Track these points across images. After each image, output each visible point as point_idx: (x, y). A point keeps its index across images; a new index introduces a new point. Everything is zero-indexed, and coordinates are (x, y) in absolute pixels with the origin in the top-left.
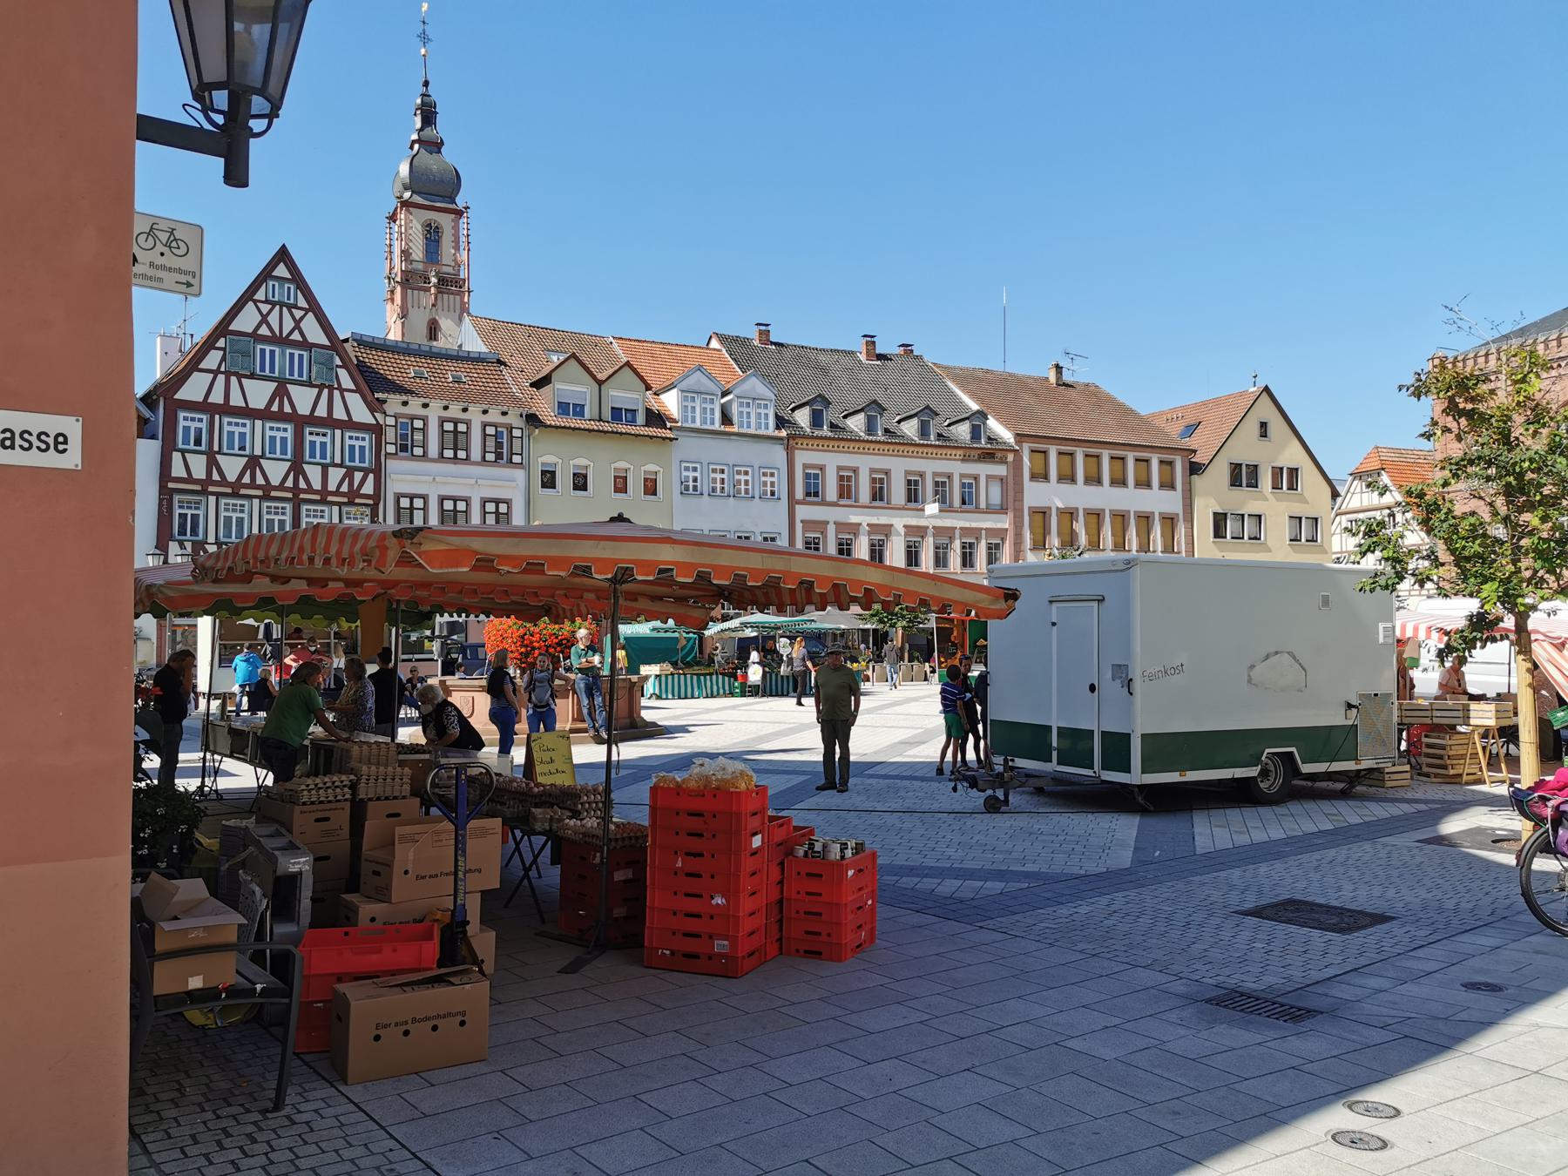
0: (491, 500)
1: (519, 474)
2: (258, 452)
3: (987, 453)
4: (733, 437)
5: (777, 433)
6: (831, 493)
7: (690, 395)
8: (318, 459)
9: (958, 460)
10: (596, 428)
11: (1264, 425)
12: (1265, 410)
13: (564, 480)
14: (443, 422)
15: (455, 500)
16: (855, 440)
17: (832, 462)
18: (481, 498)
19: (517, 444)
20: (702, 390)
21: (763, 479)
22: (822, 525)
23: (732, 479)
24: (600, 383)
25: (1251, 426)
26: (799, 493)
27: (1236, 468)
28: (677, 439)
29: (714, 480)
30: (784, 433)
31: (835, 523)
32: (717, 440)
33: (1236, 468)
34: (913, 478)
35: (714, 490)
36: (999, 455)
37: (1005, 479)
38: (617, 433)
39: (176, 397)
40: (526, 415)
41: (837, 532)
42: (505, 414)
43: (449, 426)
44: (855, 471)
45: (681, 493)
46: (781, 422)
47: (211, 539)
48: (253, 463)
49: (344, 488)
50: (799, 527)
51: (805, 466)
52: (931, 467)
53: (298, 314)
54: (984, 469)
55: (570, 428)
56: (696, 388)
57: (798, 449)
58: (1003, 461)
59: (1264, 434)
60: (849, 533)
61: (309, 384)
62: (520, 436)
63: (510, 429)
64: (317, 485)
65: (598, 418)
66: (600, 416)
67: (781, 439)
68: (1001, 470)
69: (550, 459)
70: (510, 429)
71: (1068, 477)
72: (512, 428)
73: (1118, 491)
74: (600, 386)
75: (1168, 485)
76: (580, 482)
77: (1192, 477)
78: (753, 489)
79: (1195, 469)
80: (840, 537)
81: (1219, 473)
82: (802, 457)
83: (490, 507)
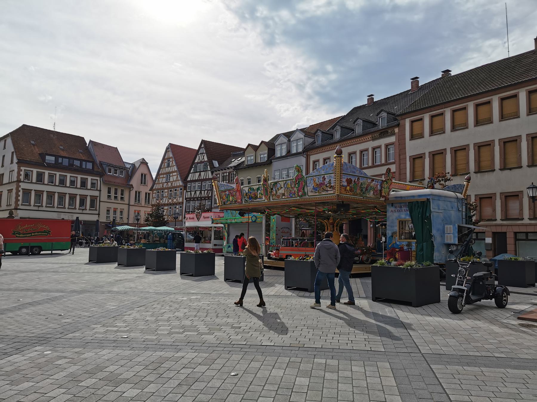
2: (196, 190)
8: (194, 190)
9: (370, 141)
20: (282, 142)
32: (282, 161)
39: (188, 180)
47: (190, 211)
48: (195, 193)
49: (207, 196)
53: (204, 154)
56: (281, 143)
57: (312, 155)
58: (393, 134)
61: (203, 171)
64: (203, 196)
74: (256, 151)
82: (313, 158)
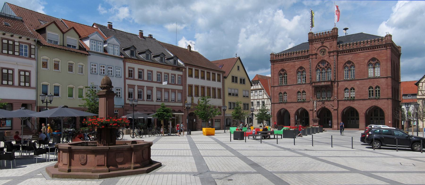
0: (22, 71)
1: (34, 62)
3: (178, 68)
4: (107, 56)
5: (120, 56)
6: (136, 77)
7: (94, 41)
10: (63, 48)
11: (238, 67)
12: (238, 63)
13: (51, 65)
14: (3, 39)
15: (8, 69)
16: (143, 61)
17: (137, 67)
18: (19, 70)
19: (33, 51)
20: (98, 40)
21: (117, 70)
22: (132, 86)
23: (107, 69)
24: (63, 33)
25: (236, 68)
26: (127, 76)
27: (233, 77)
28: (90, 55)
29: (101, 70)
30: (123, 57)
31: (137, 86)
33: (233, 77)
34: (159, 74)
35: (101, 73)
36: (181, 69)
37: (182, 76)
38: (70, 51)
40: (37, 41)
41: (138, 88)
42: (28, 39)
43: (5, 41)
44: (143, 70)
45: (91, 73)
46: (121, 54)
50: (127, 86)
51: (129, 68)
52: (164, 71)
54: (177, 73)
55: (53, 47)
58: (182, 71)
59: (238, 69)
60: (141, 89)
62: (34, 48)
63: (30, 45)
65: (63, 45)
66: (63, 45)
67: (122, 58)
68: (181, 73)
69: (46, 57)
70: (30, 45)
71: (197, 77)
72: (31, 45)
73: (208, 81)
75: (219, 80)
76: (56, 66)
77: (224, 79)
78: (113, 74)
79: (225, 77)
80: (138, 90)
81: (229, 79)
83: (22, 73)
